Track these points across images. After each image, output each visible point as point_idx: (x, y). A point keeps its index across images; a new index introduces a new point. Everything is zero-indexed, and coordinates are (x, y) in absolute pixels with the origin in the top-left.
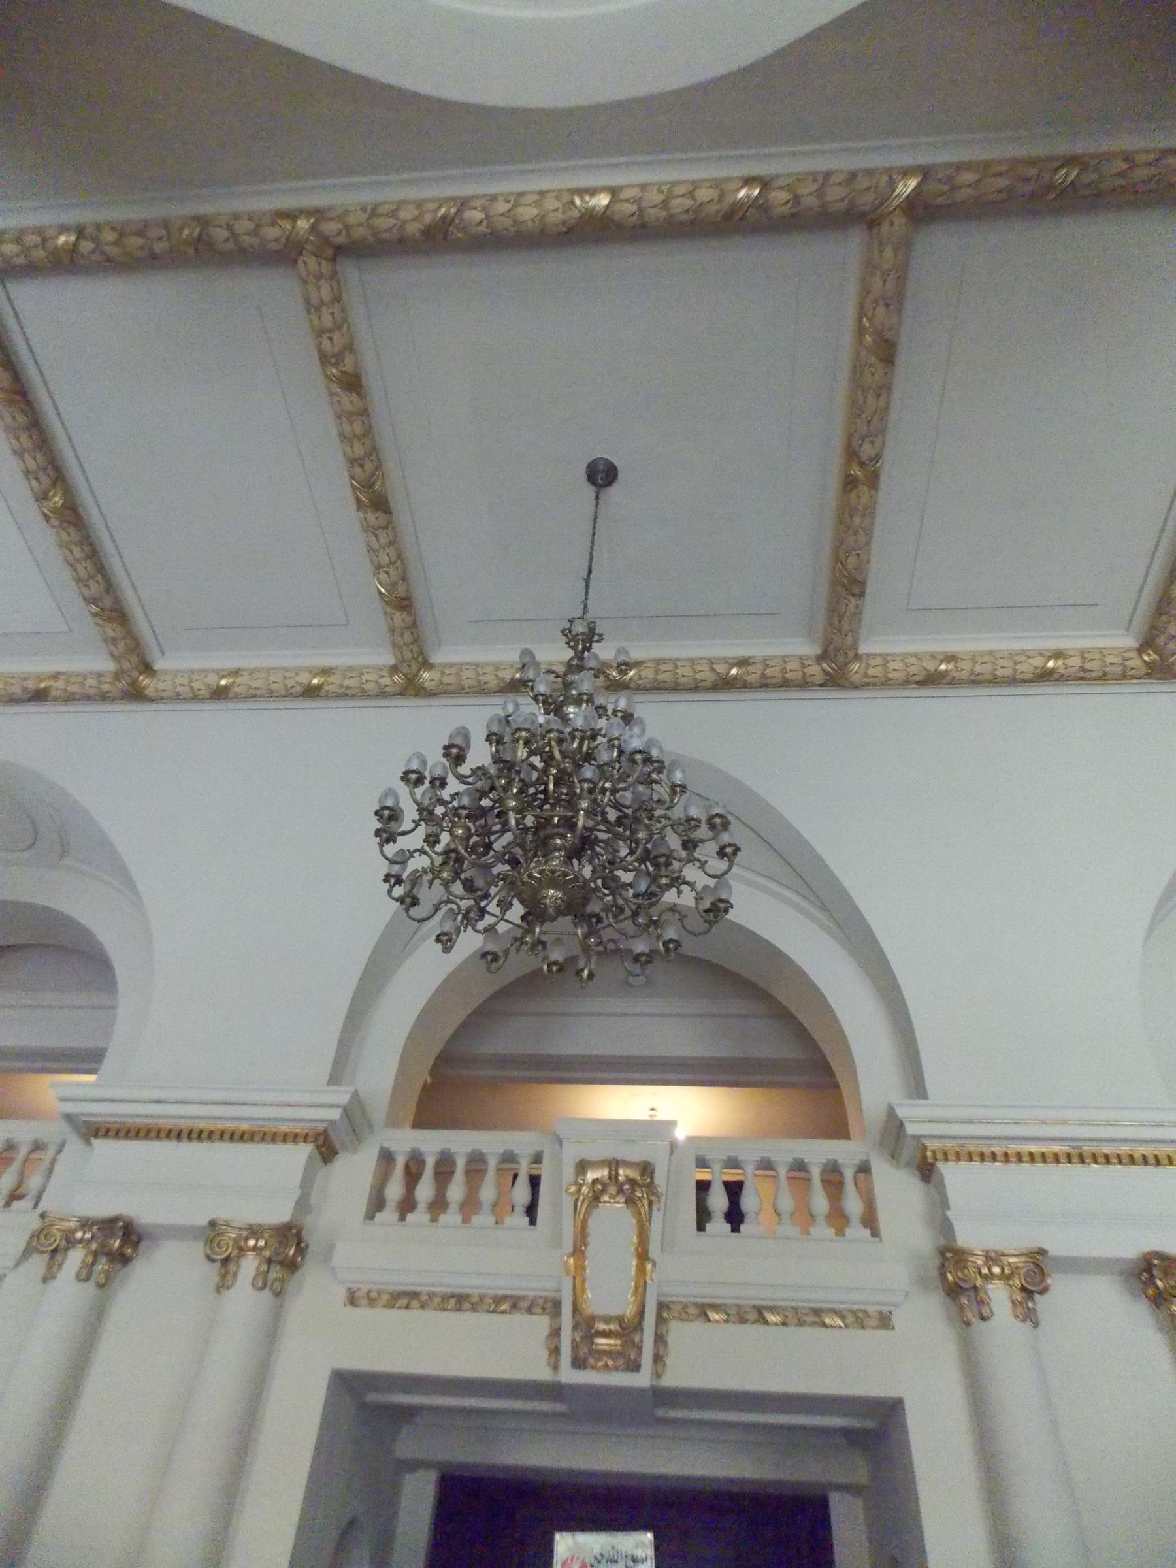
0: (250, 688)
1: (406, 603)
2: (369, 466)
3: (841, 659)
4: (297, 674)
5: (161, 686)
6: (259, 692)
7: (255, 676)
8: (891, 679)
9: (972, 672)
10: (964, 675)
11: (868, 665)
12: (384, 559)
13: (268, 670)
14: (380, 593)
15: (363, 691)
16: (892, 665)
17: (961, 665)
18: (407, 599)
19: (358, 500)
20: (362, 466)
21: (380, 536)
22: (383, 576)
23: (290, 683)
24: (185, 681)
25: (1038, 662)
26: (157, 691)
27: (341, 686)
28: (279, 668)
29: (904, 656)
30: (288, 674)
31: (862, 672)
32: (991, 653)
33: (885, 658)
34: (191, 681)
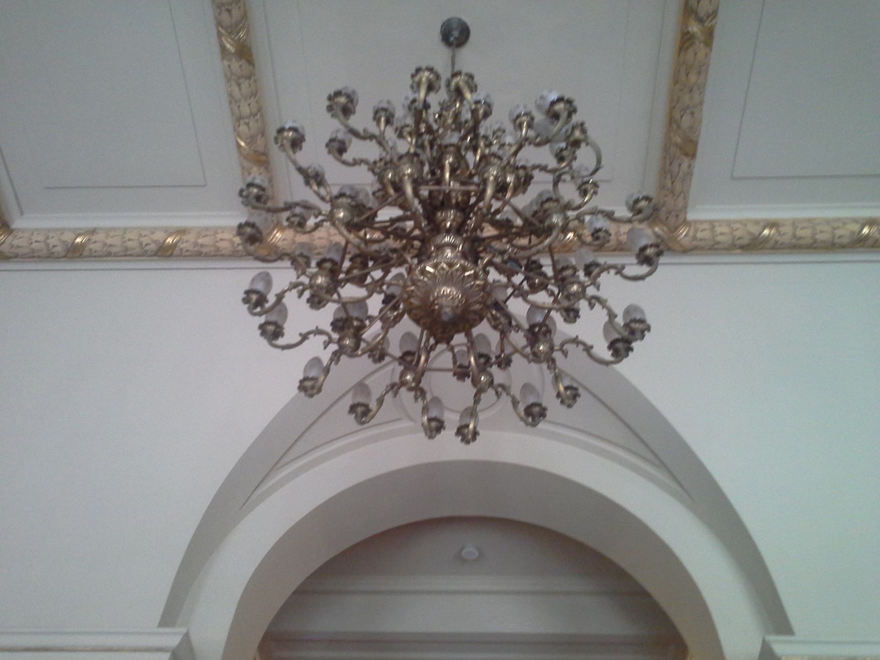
0: (105, 245)
1: (263, 158)
2: (236, 13)
3: (672, 220)
4: (153, 233)
5: (16, 242)
6: (113, 250)
7: (112, 234)
8: (718, 243)
9: (794, 236)
10: (786, 239)
11: (696, 231)
12: (246, 110)
13: (125, 230)
14: (239, 146)
15: (218, 249)
16: (719, 230)
17: (783, 230)
18: (265, 154)
19: (223, 48)
20: (229, 11)
21: (243, 86)
22: (243, 128)
23: (145, 240)
24: (41, 238)
25: (855, 227)
26: (12, 246)
27: (196, 244)
28: (136, 228)
29: (729, 223)
30: (143, 233)
31: (691, 234)
32: (810, 220)
33: (712, 223)
34: (47, 238)
